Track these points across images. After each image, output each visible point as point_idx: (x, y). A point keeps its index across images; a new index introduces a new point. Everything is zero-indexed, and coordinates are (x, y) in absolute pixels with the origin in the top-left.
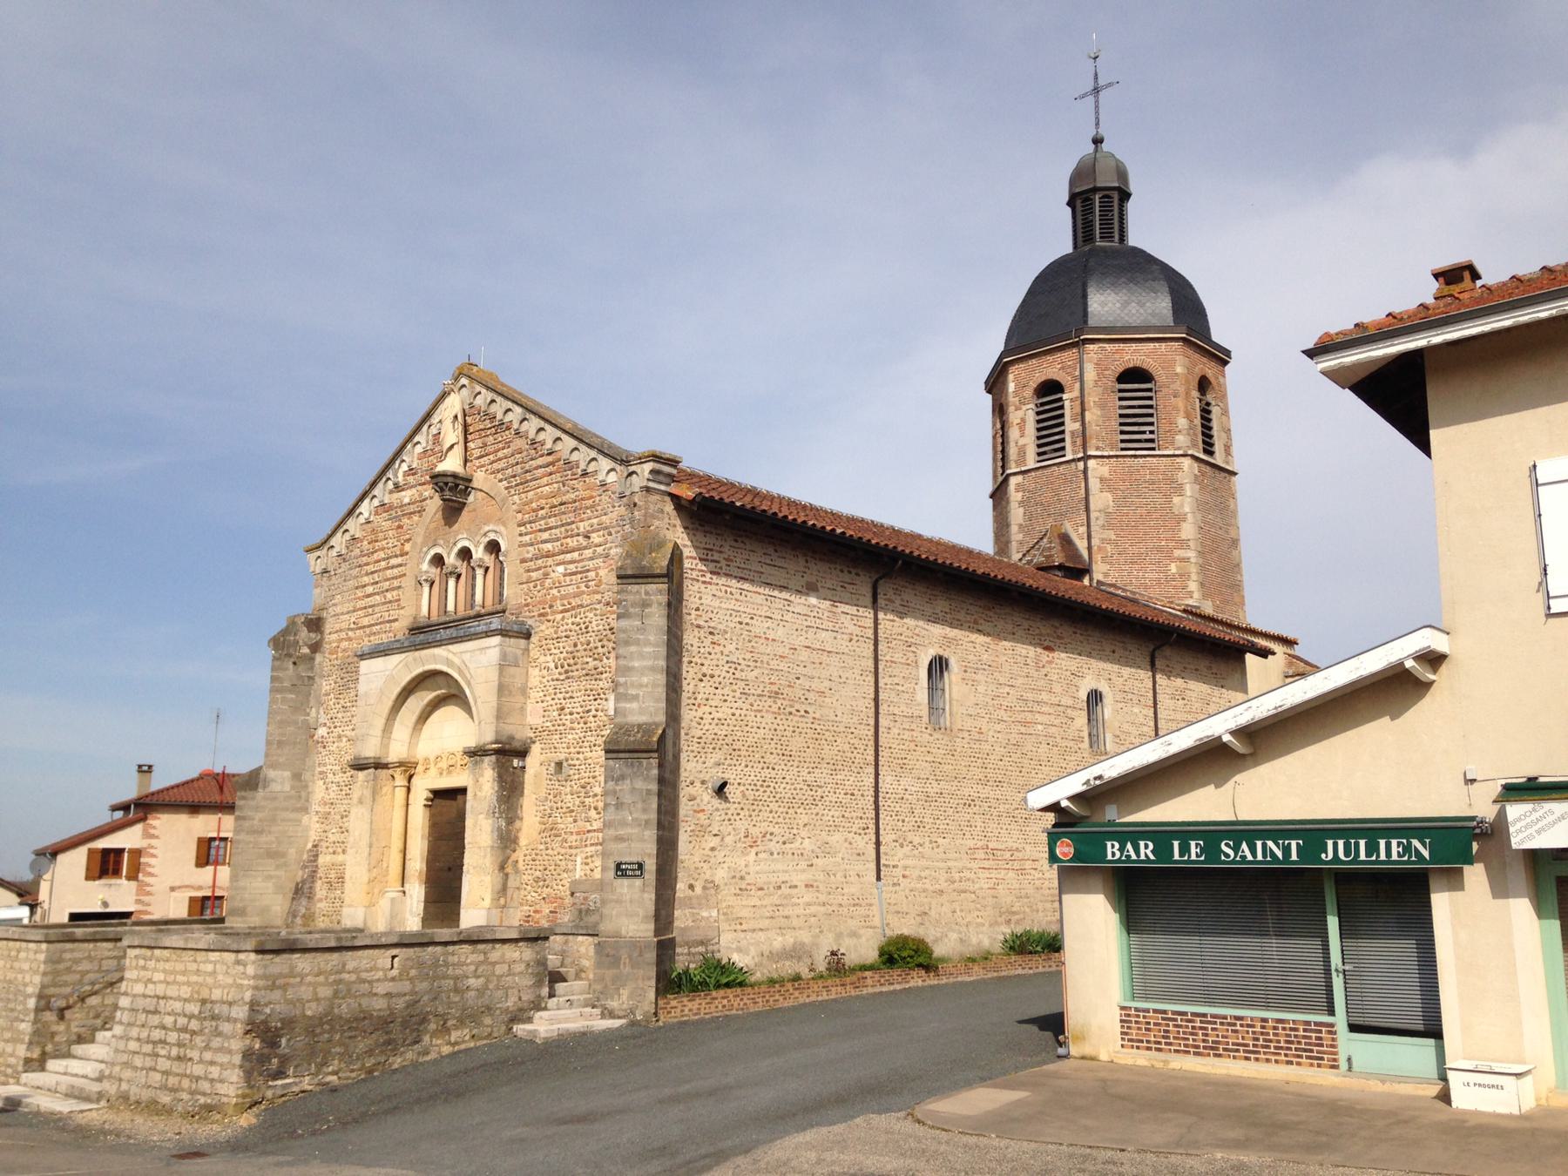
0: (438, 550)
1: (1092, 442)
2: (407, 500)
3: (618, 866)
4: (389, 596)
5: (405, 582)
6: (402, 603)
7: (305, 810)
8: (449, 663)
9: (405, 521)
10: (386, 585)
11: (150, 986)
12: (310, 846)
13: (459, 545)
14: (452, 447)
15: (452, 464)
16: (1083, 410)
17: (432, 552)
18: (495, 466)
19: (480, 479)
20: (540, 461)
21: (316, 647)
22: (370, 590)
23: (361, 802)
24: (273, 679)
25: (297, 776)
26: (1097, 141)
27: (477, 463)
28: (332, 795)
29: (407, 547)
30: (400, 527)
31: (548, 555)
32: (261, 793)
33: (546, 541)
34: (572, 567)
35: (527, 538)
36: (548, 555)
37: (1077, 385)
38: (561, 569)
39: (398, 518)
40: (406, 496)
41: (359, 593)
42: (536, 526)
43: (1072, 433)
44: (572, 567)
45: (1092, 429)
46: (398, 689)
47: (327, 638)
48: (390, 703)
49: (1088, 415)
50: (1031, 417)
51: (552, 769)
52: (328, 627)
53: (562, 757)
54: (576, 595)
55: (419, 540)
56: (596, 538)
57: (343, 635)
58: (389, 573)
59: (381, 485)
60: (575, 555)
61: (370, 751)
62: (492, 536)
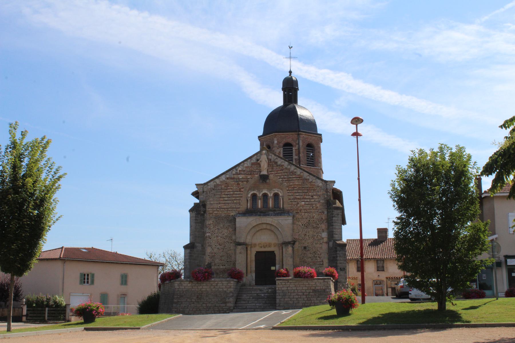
0: (255, 192)
1: (301, 163)
3: (340, 269)
4: (235, 201)
5: (241, 198)
7: (204, 254)
9: (240, 183)
10: (234, 199)
12: (206, 264)
15: (264, 172)
16: (299, 153)
17: (252, 192)
19: (271, 176)
20: (294, 176)
21: (205, 212)
22: (227, 199)
23: (240, 253)
24: (196, 220)
25: (202, 246)
26: (290, 72)
28: (215, 251)
29: (242, 190)
31: (298, 199)
32: (195, 250)
34: (307, 203)
35: (291, 194)
37: (297, 146)
38: (303, 203)
40: (241, 177)
41: (222, 199)
42: (294, 191)
43: (295, 159)
44: (307, 203)
45: (302, 159)
47: (207, 210)
49: (301, 155)
50: (282, 151)
51: (303, 248)
52: (207, 207)
54: (309, 209)
55: (248, 189)
56: (315, 197)
57: (215, 209)
58: (234, 195)
59: (230, 172)
60: (308, 200)
61: (242, 240)
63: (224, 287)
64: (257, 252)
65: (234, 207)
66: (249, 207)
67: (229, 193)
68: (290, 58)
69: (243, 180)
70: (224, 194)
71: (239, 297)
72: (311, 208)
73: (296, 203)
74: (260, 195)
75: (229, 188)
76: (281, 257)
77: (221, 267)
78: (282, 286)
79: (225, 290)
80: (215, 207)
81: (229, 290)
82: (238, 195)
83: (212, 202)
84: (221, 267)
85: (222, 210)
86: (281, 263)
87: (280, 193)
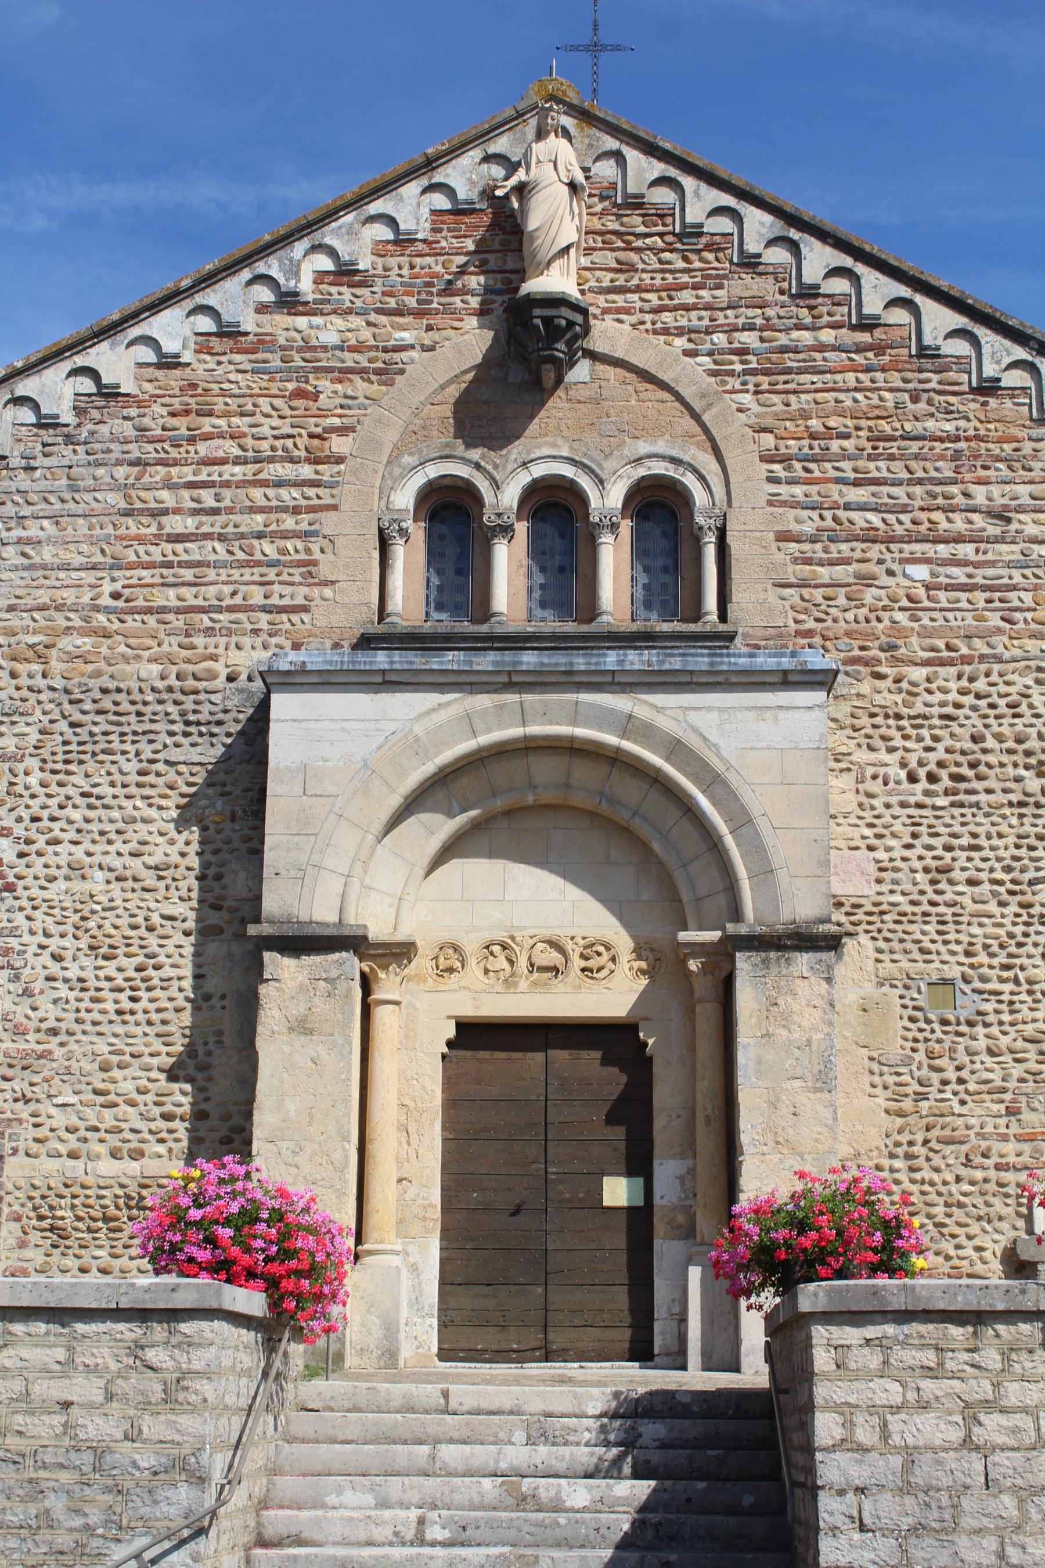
2: (330, 337)
4: (269, 549)
5: (328, 522)
6: (324, 571)
8: (628, 725)
9: (324, 384)
11: (992, 1420)
13: (539, 470)
14: (568, 248)
17: (433, 471)
18: (667, 317)
20: (827, 336)
22: (190, 524)
23: (302, 1027)
27: (601, 300)
28: (49, 1011)
29: (338, 445)
30: (300, 394)
31: (870, 537)
33: (863, 508)
34: (959, 574)
36: (870, 537)
38: (920, 572)
39: (288, 372)
40: (329, 331)
44: (959, 574)
46: (429, 768)
48: (395, 801)
53: (954, 972)
55: (391, 436)
58: (257, 493)
60: (967, 550)
62: (660, 468)
63: (84, 1389)
64: (473, 1035)
65: (258, 599)
66: (396, 602)
67: (212, 473)
68: (595, 48)
69: (350, 359)
70: (169, 485)
71: (278, 1520)
72: (994, 620)
73: (840, 572)
74: (505, 496)
75: (207, 425)
76: (707, 1084)
77: (108, 1167)
78: (890, 1392)
79: (96, 1427)
80: (69, 596)
81: (153, 1427)
82: (289, 496)
83: (47, 554)
84: (108, 1167)
85: (132, 623)
86: (707, 1141)
87: (690, 481)
